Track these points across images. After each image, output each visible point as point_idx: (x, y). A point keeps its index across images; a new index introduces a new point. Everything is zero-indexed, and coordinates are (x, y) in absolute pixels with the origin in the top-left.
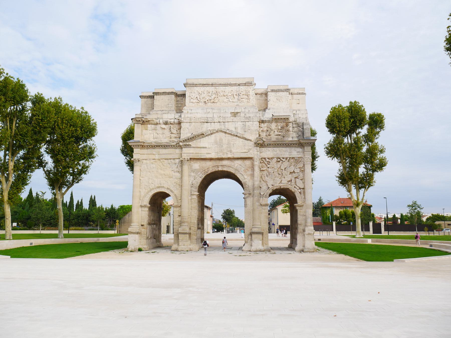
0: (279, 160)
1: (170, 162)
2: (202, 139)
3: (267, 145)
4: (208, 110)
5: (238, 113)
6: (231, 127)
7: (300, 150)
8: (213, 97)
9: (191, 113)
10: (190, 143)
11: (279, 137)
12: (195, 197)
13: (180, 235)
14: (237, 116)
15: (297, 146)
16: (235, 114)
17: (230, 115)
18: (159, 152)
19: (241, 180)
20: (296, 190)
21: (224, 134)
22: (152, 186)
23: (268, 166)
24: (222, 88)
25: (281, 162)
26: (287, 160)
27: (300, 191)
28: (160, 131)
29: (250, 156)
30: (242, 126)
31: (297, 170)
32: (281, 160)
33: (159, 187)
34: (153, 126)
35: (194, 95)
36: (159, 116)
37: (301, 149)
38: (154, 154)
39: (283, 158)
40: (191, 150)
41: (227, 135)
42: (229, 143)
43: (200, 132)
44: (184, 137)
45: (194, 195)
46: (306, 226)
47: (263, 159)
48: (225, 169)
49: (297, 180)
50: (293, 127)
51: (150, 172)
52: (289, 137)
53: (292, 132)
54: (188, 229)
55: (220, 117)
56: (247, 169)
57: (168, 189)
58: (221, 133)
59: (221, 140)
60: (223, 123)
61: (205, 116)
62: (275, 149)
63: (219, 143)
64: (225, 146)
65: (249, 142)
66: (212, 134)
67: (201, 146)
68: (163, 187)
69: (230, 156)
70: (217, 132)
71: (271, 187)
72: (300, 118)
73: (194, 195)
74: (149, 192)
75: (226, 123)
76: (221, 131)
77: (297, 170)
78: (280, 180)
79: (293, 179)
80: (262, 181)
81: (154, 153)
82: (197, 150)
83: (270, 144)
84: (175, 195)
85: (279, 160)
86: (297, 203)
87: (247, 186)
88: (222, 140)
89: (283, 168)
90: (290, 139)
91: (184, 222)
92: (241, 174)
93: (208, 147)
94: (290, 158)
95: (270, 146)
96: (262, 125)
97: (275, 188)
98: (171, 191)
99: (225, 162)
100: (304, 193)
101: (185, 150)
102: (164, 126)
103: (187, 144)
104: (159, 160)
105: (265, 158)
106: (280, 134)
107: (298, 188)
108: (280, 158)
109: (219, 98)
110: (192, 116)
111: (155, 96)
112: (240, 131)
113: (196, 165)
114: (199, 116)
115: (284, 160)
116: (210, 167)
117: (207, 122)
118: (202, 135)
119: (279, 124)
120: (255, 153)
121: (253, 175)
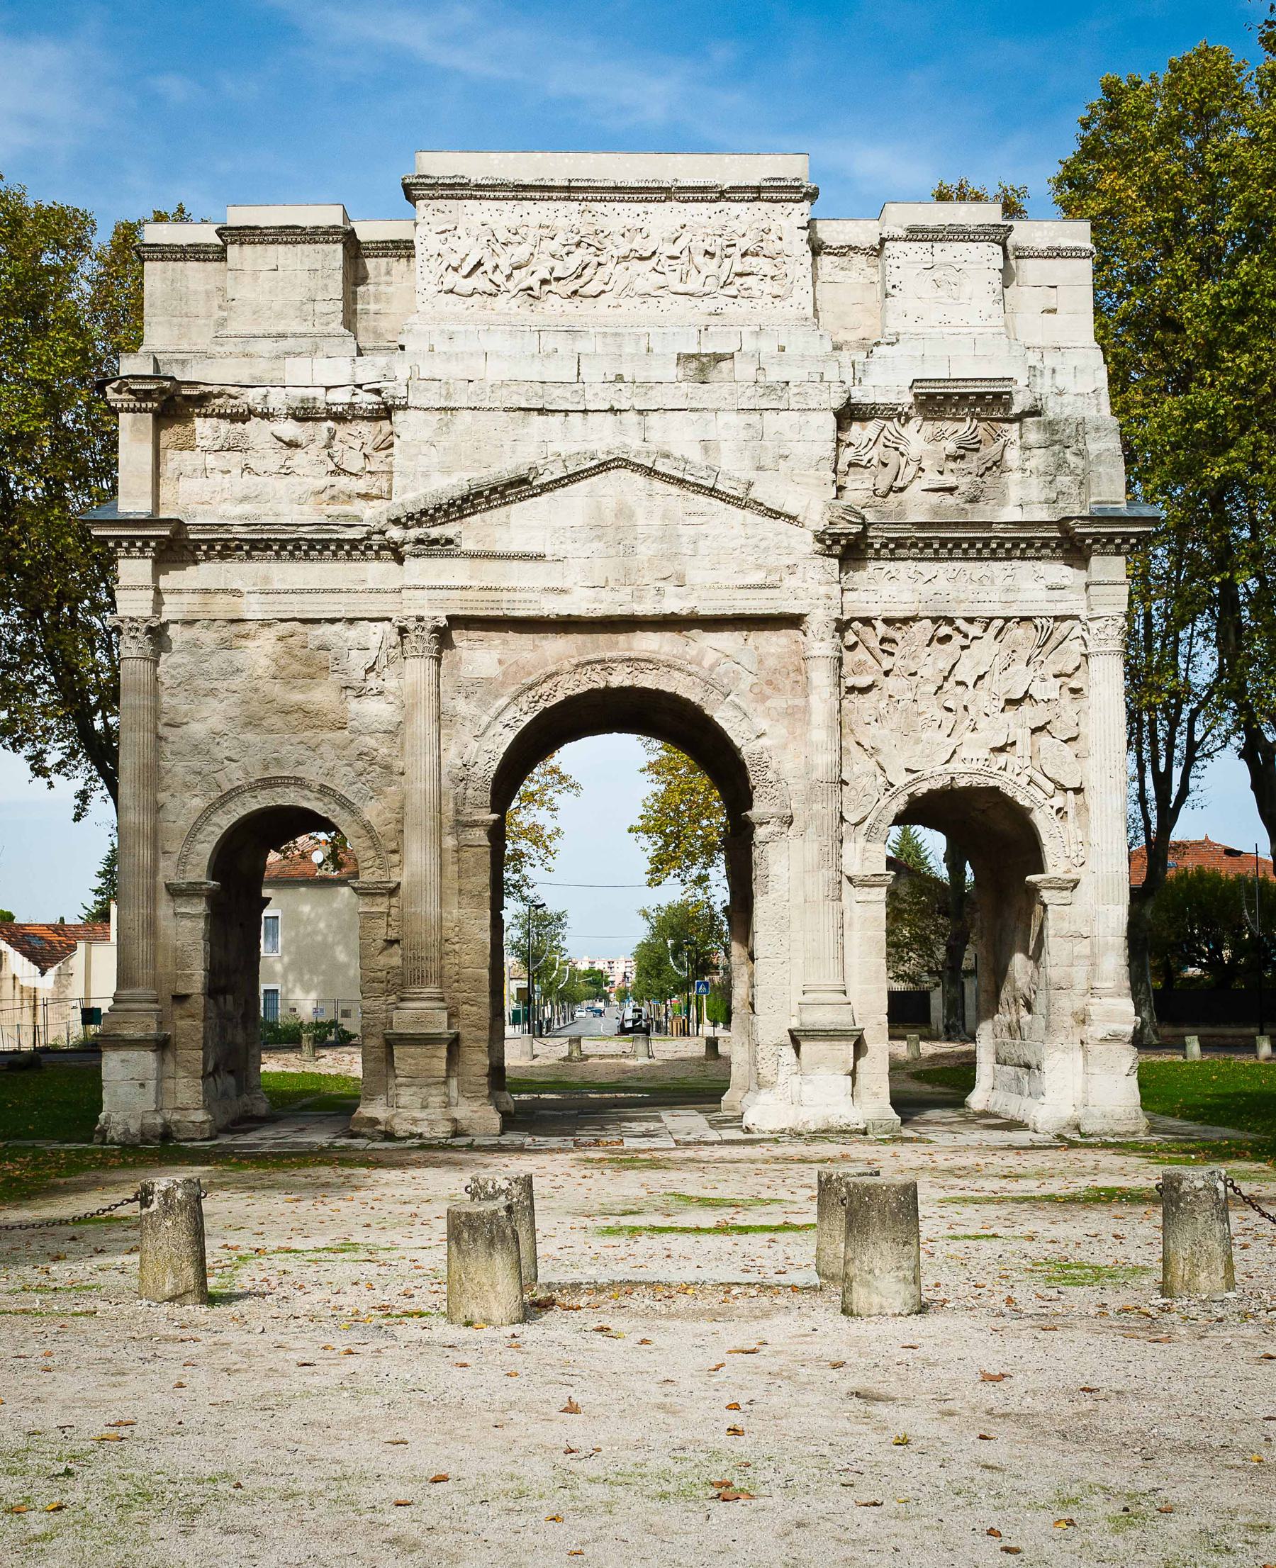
0: (945, 630)
3: (884, 546)
4: (549, 342)
5: (718, 358)
6: (678, 439)
7: (1058, 571)
8: (573, 262)
9: (448, 357)
10: (449, 530)
11: (949, 500)
12: (479, 836)
13: (398, 1051)
14: (713, 375)
15: (1047, 552)
16: (703, 365)
17: (673, 371)
18: (267, 579)
19: (738, 742)
20: (1040, 796)
21: (639, 479)
22: (234, 776)
23: (887, 663)
25: (958, 640)
26: (992, 631)
27: (1058, 801)
28: (273, 459)
29: (793, 608)
30: (744, 434)
31: (1046, 689)
32: (957, 629)
33: (268, 783)
34: (225, 425)
35: (463, 246)
36: (261, 369)
37: (1068, 570)
39: (970, 620)
41: (658, 485)
42: (668, 533)
43: (504, 468)
44: (410, 496)
45: (475, 824)
47: (856, 625)
48: (648, 681)
49: (1043, 738)
50: (1025, 448)
52: (1002, 501)
53: (1017, 476)
54: (444, 1016)
55: (620, 378)
56: (769, 683)
57: (324, 790)
58: (624, 473)
59: (624, 513)
60: (631, 417)
61: (534, 371)
62: (923, 566)
63: (615, 532)
64: (645, 551)
65: (780, 524)
66: (573, 478)
67: (515, 548)
68: (298, 782)
69: (673, 604)
70: (603, 467)
71: (901, 779)
72: (1061, 393)
73: (475, 824)
74: (212, 809)
75: (653, 418)
76: (623, 463)
77: (1046, 689)
78: (954, 741)
79: (1022, 736)
80: (854, 749)
82: (491, 573)
83: (900, 543)
84: (367, 827)
85: (945, 630)
86: (1040, 869)
87: (770, 775)
88: (631, 515)
89: (966, 672)
90: (1011, 513)
91: (421, 979)
92: (737, 707)
93: (555, 555)
94: (1007, 620)
95: (902, 552)
96: (857, 432)
97: (923, 788)
98: (344, 803)
100: (1083, 809)
101: (418, 570)
102: (289, 429)
103: (435, 532)
105: (867, 621)
106: (950, 480)
107: (1050, 787)
108: (950, 621)
109: (610, 265)
110: (456, 370)
111: (232, 251)
112: (733, 469)
114: (495, 371)
115: (974, 630)
116: (566, 667)
117: (541, 411)
118: (517, 487)
119: (949, 426)
121: (798, 715)
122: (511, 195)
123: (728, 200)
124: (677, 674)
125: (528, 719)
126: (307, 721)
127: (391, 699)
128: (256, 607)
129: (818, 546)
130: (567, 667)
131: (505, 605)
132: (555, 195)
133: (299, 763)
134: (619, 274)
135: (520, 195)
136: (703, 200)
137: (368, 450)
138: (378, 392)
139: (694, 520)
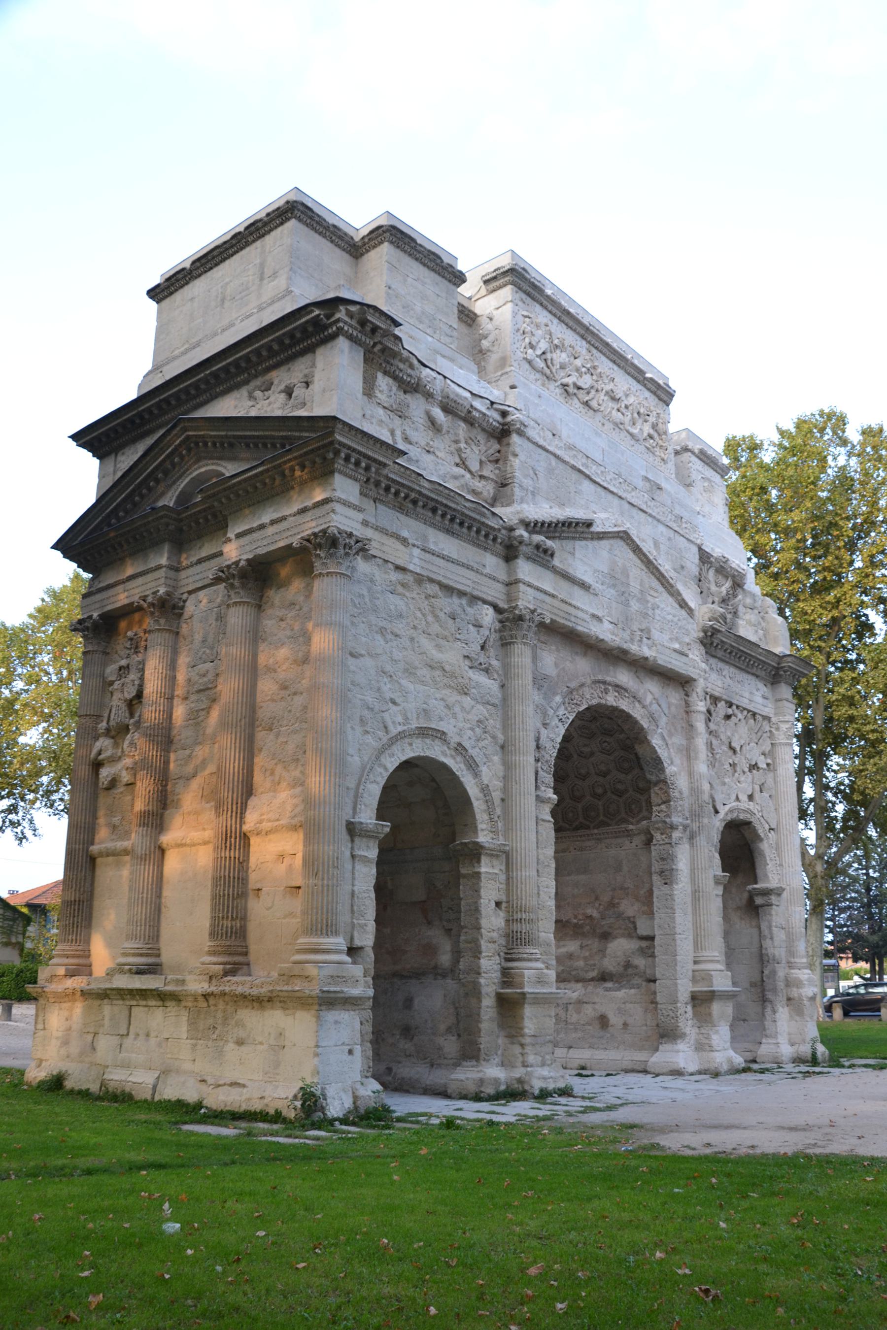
1: (459, 611)
2: (578, 543)
18: (425, 538)
24: (605, 365)
38: (404, 541)
40: (547, 582)
46: (791, 965)
48: (623, 705)
51: (382, 631)
59: (625, 572)
76: (624, 537)
81: (405, 534)
82: (563, 589)
84: (485, 790)
87: (677, 794)
99: (624, 677)
102: (438, 413)
104: (420, 579)
113: (553, 659)
120: (695, 663)
122: (559, 314)
123: (645, 386)
124: (637, 704)
125: (571, 718)
126: (446, 681)
127: (496, 676)
128: (416, 560)
129: (701, 634)
130: (589, 682)
131: (573, 619)
132: (579, 329)
133: (441, 719)
134: (609, 406)
135: (564, 318)
136: (635, 378)
137: (484, 459)
138: (504, 414)
139: (652, 593)
